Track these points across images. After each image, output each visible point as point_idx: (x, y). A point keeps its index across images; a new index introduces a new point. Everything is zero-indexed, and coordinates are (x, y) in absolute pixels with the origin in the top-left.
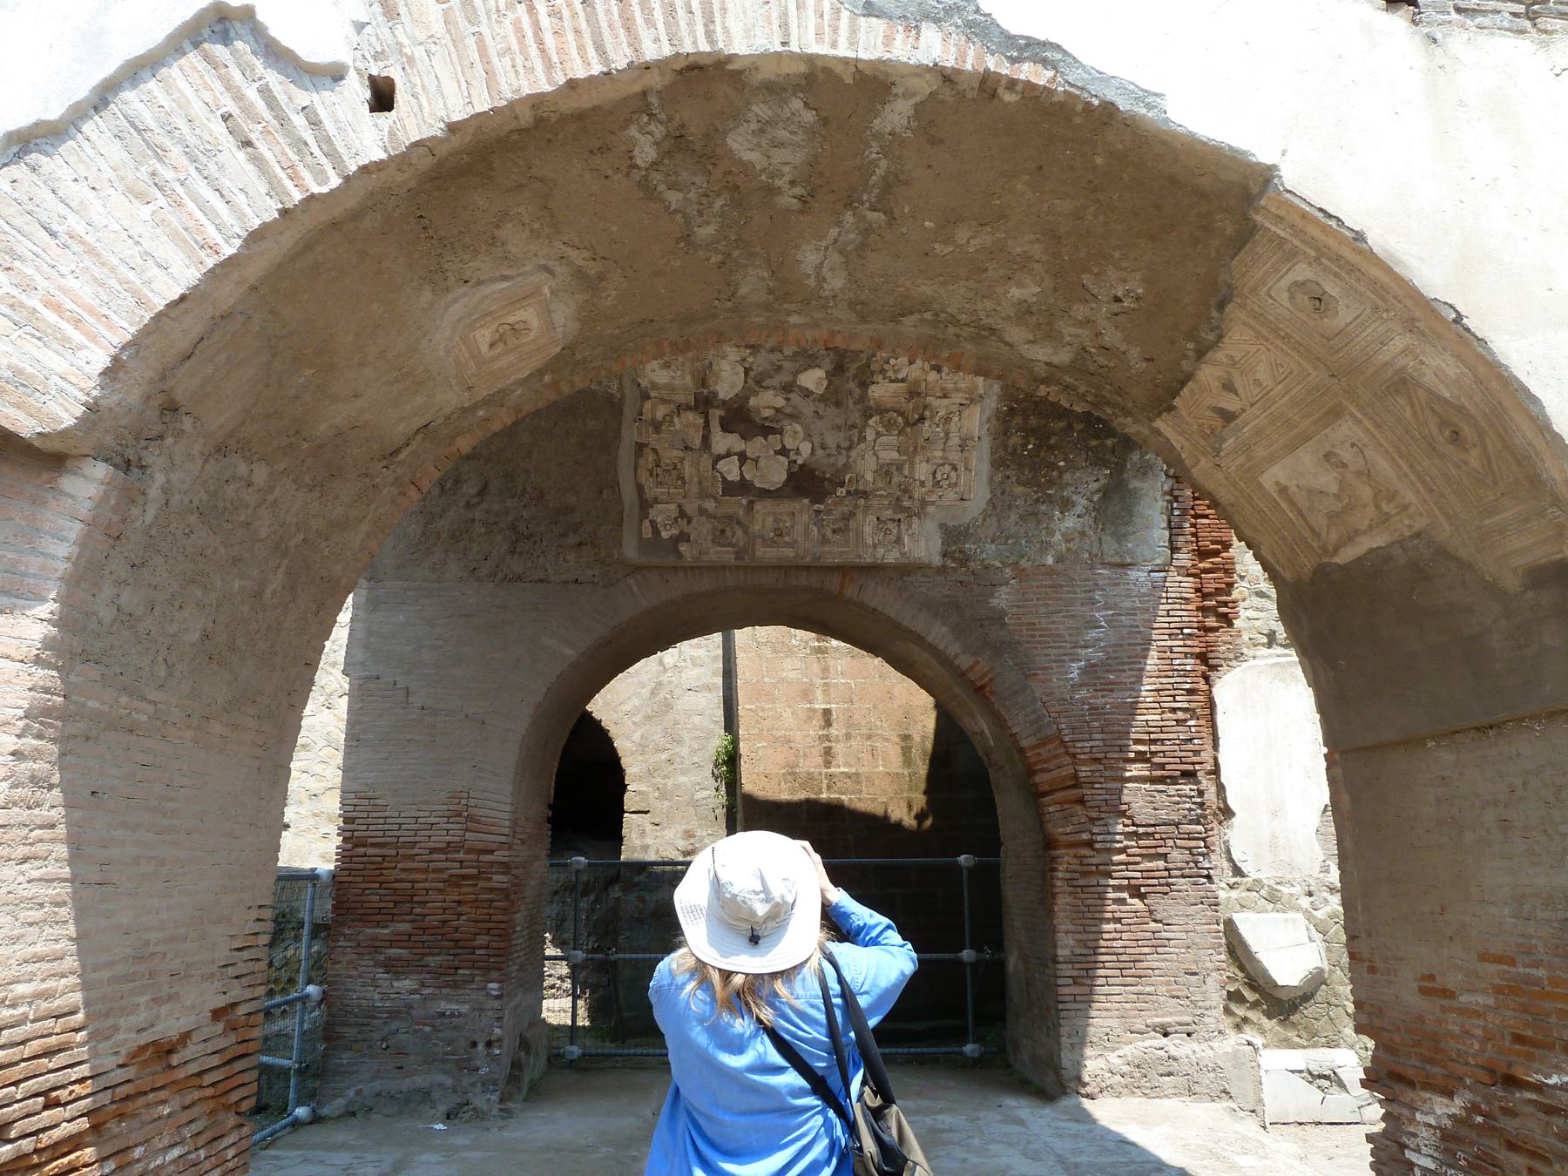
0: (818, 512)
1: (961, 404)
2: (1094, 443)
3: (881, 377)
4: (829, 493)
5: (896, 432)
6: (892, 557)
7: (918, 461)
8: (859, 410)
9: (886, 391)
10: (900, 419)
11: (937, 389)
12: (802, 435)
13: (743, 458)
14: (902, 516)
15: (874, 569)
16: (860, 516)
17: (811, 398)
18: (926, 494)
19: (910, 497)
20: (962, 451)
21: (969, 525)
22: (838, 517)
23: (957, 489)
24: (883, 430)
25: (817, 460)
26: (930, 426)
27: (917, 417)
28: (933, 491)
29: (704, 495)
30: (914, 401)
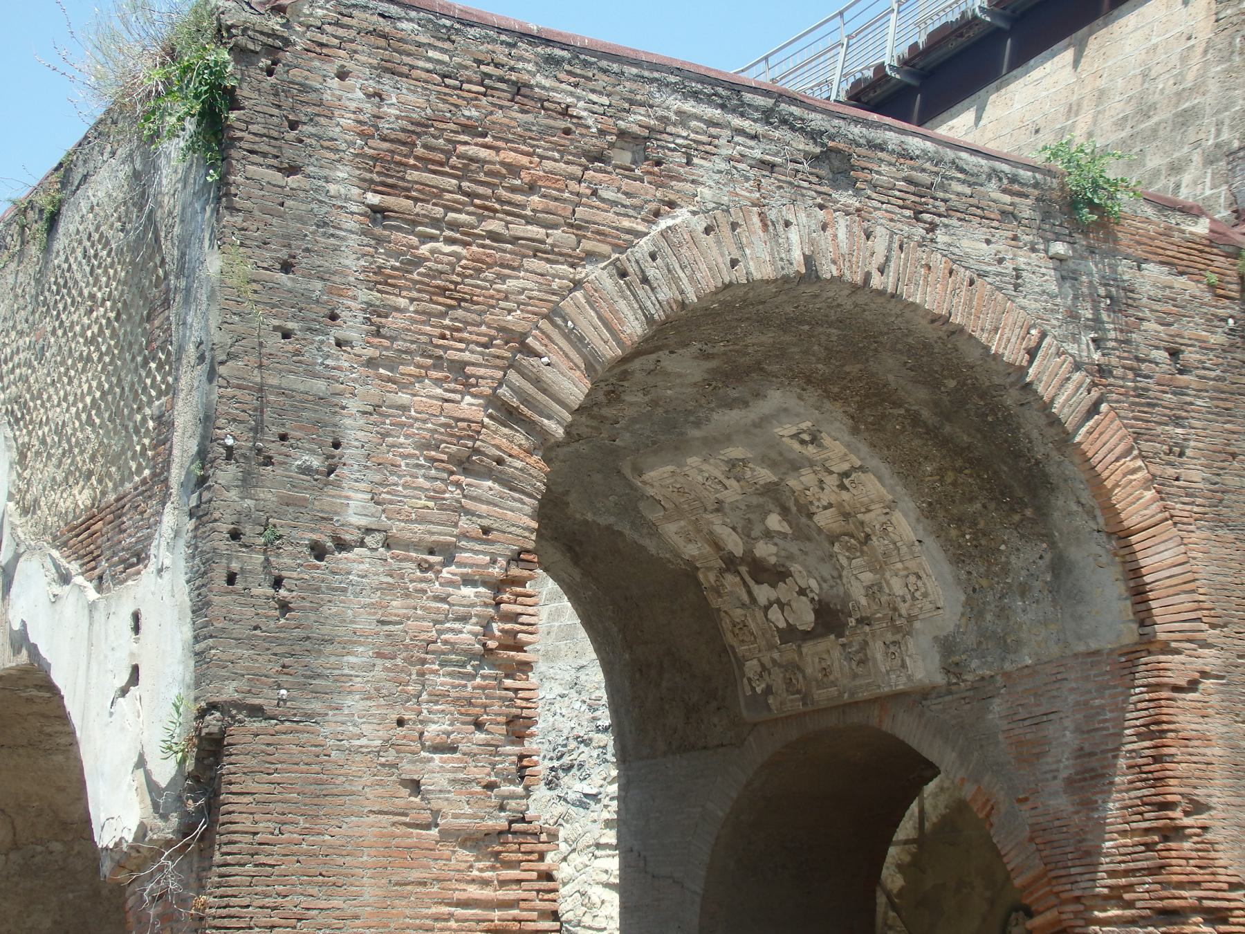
0: (843, 645)
2: (1017, 518)
6: (901, 684)
13: (782, 606)
14: (898, 637)
15: (898, 696)
16: (871, 643)
29: (771, 647)
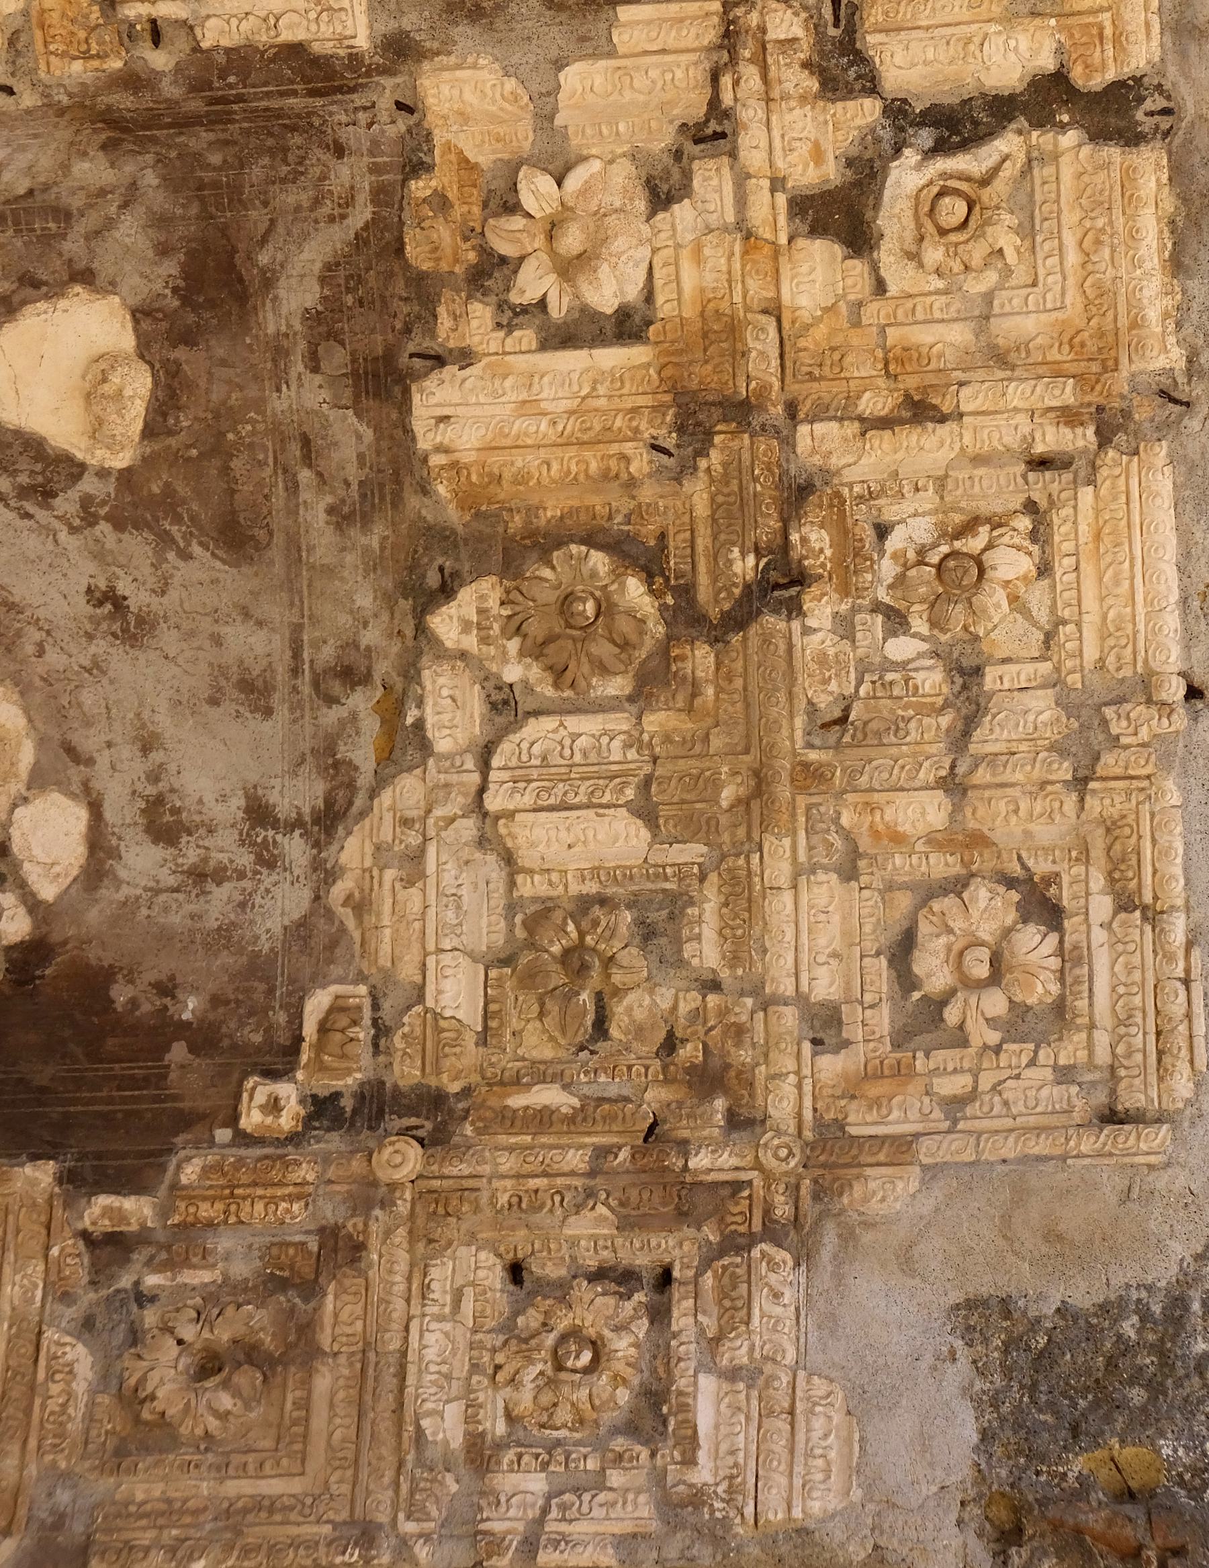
1: (1042, 463)
3: (481, 313)
4: (186, 1121)
5: (617, 686)
7: (778, 869)
8: (373, 565)
9: (528, 407)
10: (634, 590)
11: (863, 368)
12: (27, 756)
17: (67, 503)
18: (852, 1090)
19: (737, 1122)
20: (1080, 783)
21: (1177, 1303)
22: (241, 1269)
23: (1070, 1051)
24: (535, 672)
25: (129, 906)
26: (845, 627)
27: (745, 566)
28: (902, 1073)
30: (715, 457)
